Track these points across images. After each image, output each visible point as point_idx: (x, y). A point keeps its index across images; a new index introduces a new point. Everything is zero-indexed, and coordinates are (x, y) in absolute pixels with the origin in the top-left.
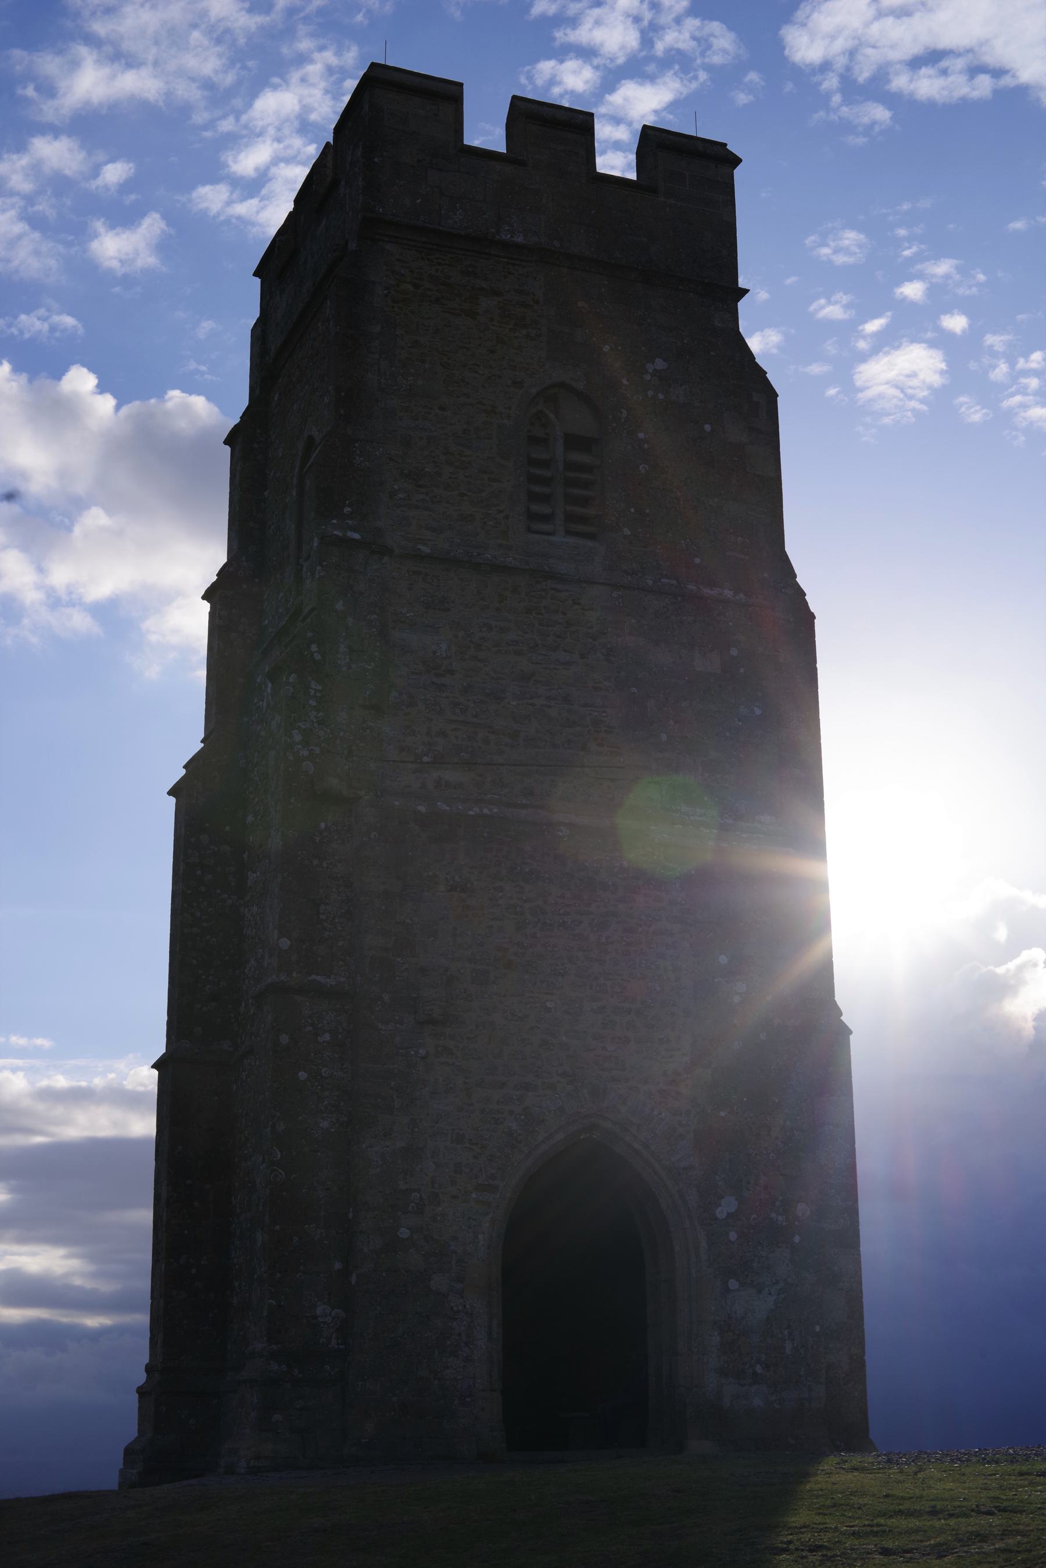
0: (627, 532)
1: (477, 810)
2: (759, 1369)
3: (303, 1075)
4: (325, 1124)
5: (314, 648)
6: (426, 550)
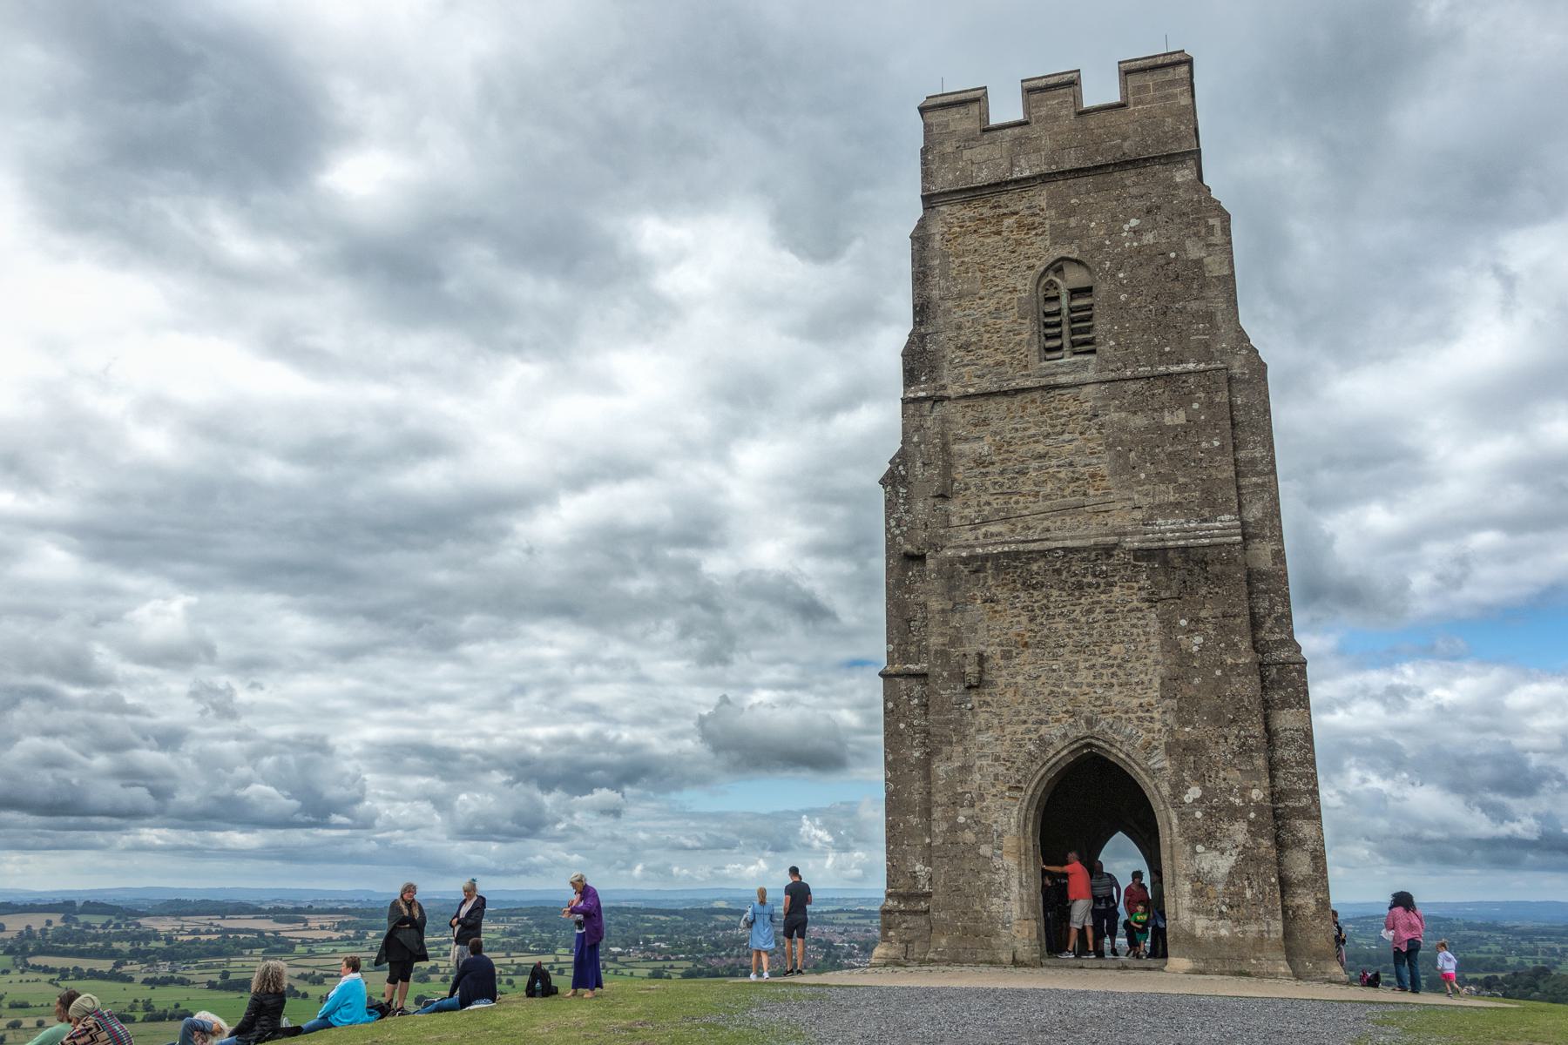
0: (1112, 343)
2: (1224, 908)
3: (902, 726)
4: (917, 754)
6: (971, 390)
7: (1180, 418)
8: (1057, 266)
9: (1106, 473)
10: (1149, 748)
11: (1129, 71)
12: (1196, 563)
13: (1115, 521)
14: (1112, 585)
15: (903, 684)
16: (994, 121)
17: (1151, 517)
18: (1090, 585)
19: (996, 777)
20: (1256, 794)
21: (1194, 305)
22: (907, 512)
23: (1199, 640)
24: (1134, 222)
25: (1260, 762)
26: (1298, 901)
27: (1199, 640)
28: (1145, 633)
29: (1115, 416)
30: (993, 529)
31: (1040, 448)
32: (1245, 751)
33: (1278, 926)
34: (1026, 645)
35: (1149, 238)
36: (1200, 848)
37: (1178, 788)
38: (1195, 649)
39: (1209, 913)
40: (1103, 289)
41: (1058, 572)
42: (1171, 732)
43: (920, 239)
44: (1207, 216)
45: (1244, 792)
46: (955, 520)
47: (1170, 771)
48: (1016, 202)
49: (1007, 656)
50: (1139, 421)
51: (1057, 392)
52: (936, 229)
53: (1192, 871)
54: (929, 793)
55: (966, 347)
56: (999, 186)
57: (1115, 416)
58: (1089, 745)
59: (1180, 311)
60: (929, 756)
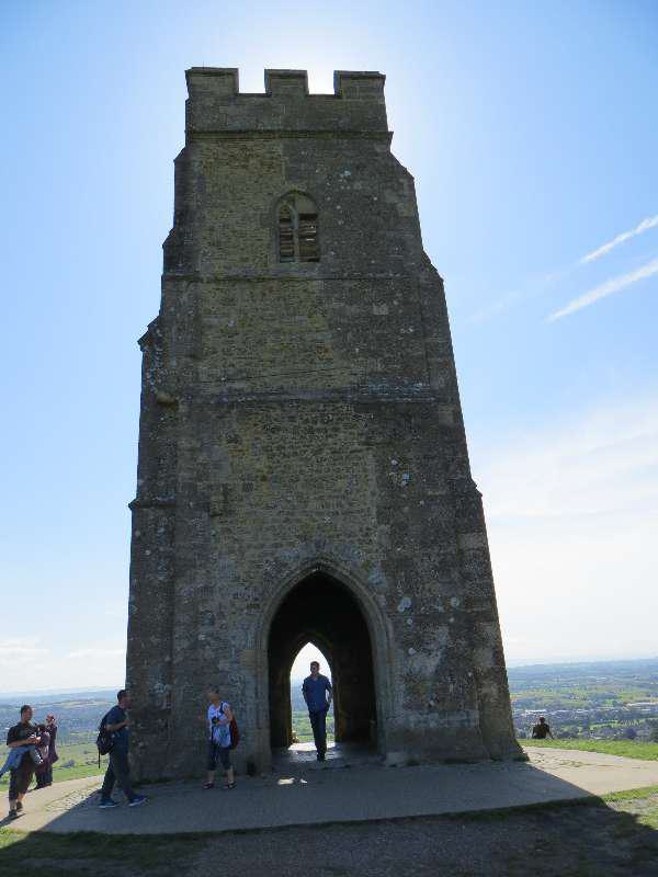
1: (243, 399)
2: (432, 703)
5: (158, 331)
7: (382, 310)
8: (290, 197)
9: (329, 346)
10: (368, 566)
11: (341, 77)
12: (403, 415)
13: (337, 384)
14: (337, 430)
15: (151, 514)
16: (242, 90)
17: (364, 382)
18: (318, 430)
19: (235, 596)
20: (454, 602)
21: (391, 234)
22: (162, 367)
23: (406, 476)
24: (347, 173)
25: (455, 575)
26: (484, 690)
27: (406, 476)
28: (365, 470)
29: (335, 305)
30: (237, 385)
31: (277, 325)
32: (444, 567)
33: (476, 715)
34: (264, 479)
35: (358, 185)
36: (411, 651)
37: (393, 600)
38: (404, 483)
39: (419, 707)
40: (325, 214)
41: (292, 419)
42: (387, 552)
43: (182, 163)
44: (399, 180)
45: (446, 600)
46: (203, 378)
47: (385, 585)
48: (258, 147)
49: (247, 488)
50: (353, 310)
51: (291, 283)
52: (195, 158)
53: (406, 671)
54: (172, 614)
55: (217, 244)
56: (244, 134)
57: (335, 305)
58: (319, 565)
59: (383, 237)
60: (173, 579)
